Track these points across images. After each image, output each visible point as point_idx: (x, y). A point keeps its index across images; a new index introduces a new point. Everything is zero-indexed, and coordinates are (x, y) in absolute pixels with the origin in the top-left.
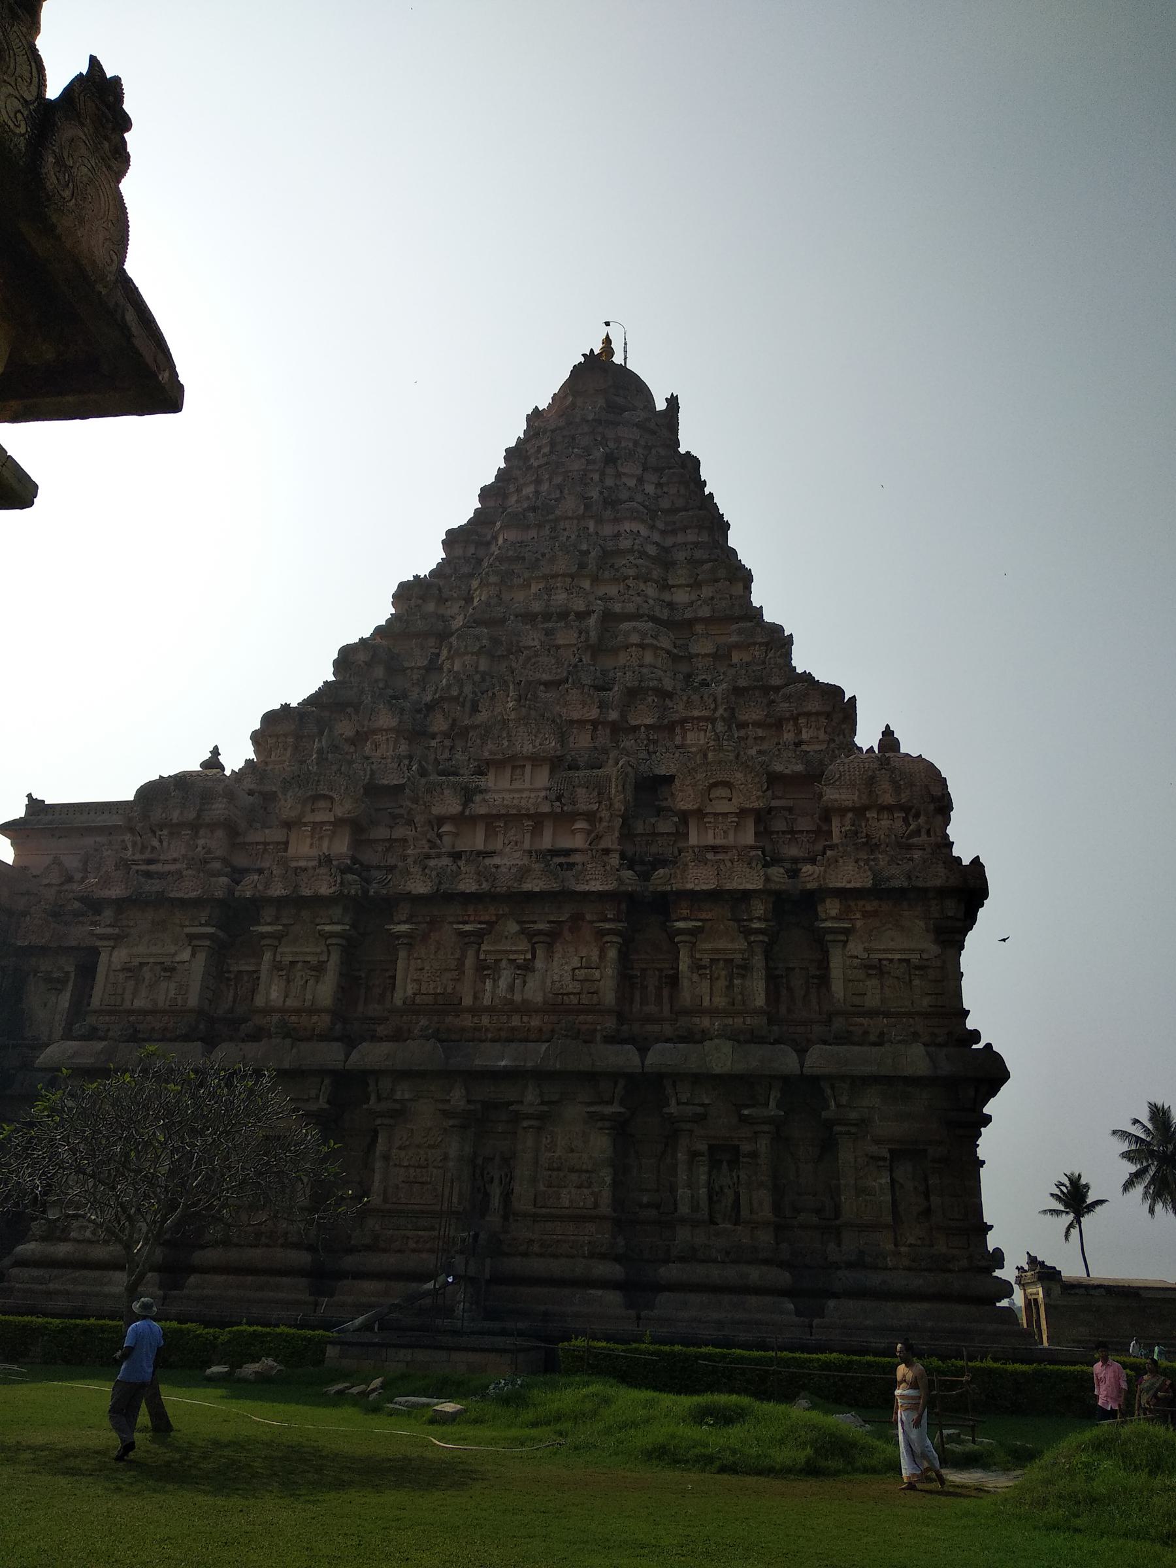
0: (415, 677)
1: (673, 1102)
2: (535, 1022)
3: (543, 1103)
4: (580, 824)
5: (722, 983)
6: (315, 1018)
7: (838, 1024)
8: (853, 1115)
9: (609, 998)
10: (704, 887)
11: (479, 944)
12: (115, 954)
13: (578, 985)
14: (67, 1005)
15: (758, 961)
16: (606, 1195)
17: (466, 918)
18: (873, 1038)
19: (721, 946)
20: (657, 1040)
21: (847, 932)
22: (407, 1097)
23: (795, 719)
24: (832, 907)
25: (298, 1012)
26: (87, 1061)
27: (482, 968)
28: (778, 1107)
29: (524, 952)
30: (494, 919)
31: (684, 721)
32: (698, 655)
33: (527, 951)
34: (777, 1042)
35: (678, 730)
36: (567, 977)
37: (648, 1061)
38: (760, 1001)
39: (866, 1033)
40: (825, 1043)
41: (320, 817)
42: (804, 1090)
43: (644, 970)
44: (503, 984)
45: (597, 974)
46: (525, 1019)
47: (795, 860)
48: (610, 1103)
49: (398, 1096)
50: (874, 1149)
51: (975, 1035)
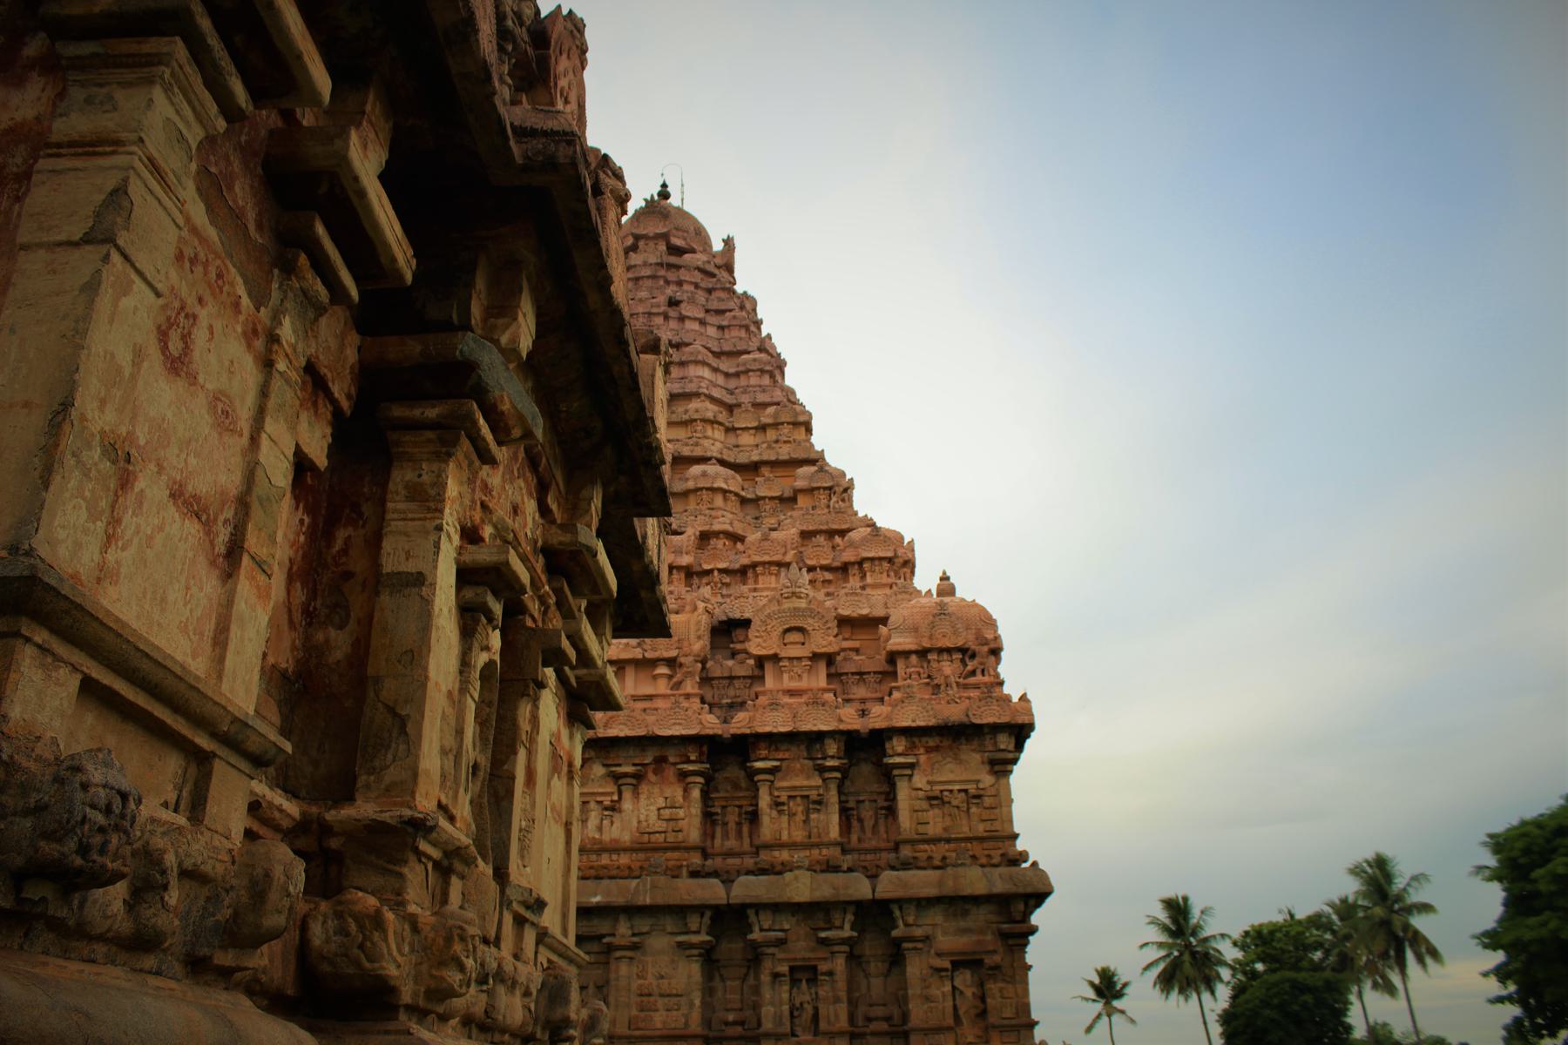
1: (757, 928)
2: (624, 859)
3: (634, 935)
4: (663, 670)
5: (800, 817)
7: (906, 852)
8: (918, 932)
9: (694, 834)
10: (782, 729)
13: (664, 824)
15: (833, 797)
16: (696, 1015)
18: (937, 862)
19: (797, 783)
20: (739, 873)
21: (912, 766)
23: (860, 563)
24: (899, 744)
28: (852, 929)
29: (612, 794)
31: (754, 566)
33: (612, 794)
34: (850, 870)
35: (750, 574)
36: (653, 817)
37: (733, 894)
38: (834, 833)
39: (930, 858)
40: (893, 868)
42: (875, 914)
43: (724, 807)
45: (681, 813)
46: (614, 857)
47: (863, 701)
48: (698, 932)
50: (938, 963)
51: (1023, 856)
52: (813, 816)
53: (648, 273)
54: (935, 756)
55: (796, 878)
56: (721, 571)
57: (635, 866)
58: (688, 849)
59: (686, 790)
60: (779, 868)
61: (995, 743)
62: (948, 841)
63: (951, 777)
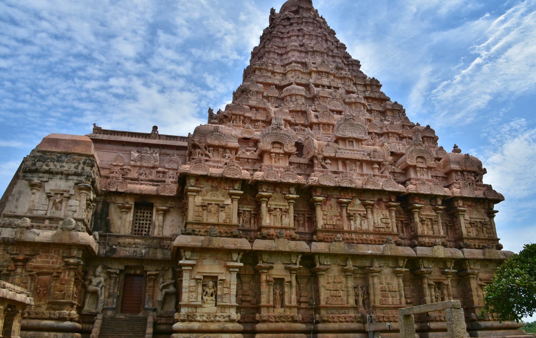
2: (372, 237)
3: (380, 267)
5: (430, 226)
6: (288, 231)
11: (347, 207)
12: (196, 198)
14: (132, 219)
18: (477, 247)
21: (464, 211)
24: (461, 203)
25: (282, 228)
26: (199, 244)
27: (349, 217)
32: (374, 110)
36: (380, 222)
37: (418, 253)
38: (442, 233)
39: (475, 245)
41: (277, 151)
44: (358, 222)
46: (368, 236)
48: (402, 267)
49: (325, 263)
50: (480, 282)
53: (311, 21)
54: (471, 209)
55: (438, 249)
56: (375, 133)
57: (377, 240)
59: (390, 212)
60: (427, 244)
61: (489, 206)
62: (479, 239)
63: (476, 217)
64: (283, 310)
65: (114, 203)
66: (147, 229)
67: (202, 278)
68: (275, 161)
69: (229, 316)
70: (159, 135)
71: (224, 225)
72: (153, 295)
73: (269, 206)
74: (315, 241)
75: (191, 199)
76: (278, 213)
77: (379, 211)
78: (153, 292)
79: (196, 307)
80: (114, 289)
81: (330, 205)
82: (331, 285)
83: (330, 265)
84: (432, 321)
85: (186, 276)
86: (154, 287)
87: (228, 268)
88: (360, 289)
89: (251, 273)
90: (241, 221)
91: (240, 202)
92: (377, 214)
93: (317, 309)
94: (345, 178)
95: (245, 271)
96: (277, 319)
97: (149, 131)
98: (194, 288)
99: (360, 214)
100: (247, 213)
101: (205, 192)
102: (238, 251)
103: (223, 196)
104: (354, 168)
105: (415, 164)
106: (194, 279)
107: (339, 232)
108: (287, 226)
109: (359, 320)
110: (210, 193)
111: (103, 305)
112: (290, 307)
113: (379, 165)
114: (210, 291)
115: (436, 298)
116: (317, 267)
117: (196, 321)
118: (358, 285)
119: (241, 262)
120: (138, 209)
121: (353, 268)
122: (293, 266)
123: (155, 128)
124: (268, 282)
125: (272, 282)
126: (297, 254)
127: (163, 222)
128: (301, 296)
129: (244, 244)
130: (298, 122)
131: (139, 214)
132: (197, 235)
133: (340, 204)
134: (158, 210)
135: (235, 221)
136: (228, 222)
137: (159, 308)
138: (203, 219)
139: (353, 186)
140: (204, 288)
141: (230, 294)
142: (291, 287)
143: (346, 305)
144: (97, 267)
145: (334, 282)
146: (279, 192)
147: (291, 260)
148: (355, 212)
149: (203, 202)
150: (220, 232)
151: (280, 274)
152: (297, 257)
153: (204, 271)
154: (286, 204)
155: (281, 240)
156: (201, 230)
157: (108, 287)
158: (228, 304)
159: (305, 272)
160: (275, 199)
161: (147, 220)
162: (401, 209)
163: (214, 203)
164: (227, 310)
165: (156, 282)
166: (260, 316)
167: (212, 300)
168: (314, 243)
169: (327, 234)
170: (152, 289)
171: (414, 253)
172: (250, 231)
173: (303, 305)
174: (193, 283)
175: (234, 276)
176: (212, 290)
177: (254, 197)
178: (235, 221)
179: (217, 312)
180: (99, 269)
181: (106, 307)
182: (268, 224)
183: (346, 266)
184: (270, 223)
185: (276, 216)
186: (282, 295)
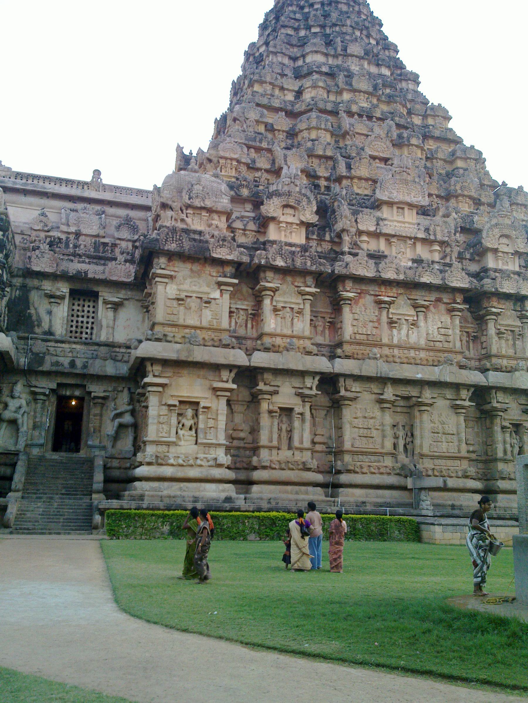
0: (281, 136)
2: (423, 355)
5: (511, 342)
6: (301, 342)
12: (168, 288)
17: (380, 293)
22: (358, 390)
25: (292, 337)
26: (173, 356)
27: (391, 323)
30: (395, 295)
36: (436, 333)
37: (490, 381)
41: (290, 219)
44: (404, 332)
46: (417, 353)
48: (465, 400)
49: (353, 390)
52: (517, 342)
55: (521, 375)
57: (430, 359)
58: (456, 352)
60: (504, 369)
64: (291, 452)
65: (38, 288)
66: (89, 331)
67: (177, 403)
68: (285, 235)
69: (216, 459)
70: (104, 185)
71: (209, 329)
72: (100, 427)
73: (274, 304)
74: (339, 357)
75: (160, 288)
76: (288, 314)
77: (437, 317)
78: (101, 423)
79: (168, 444)
80: (41, 417)
81: (364, 305)
82: (361, 420)
83: (359, 392)
84: (503, 479)
85: (153, 401)
86: (101, 415)
87: (215, 390)
88: (401, 428)
89: (248, 400)
90: (233, 324)
91: (233, 296)
92: (433, 321)
93: (338, 453)
94: (390, 265)
95: (238, 395)
96: (283, 466)
97: (88, 178)
98: (166, 417)
99: (407, 320)
100: (242, 312)
101: (181, 278)
102: (230, 367)
103: (208, 286)
104: (403, 250)
105: (496, 247)
106: (165, 404)
107: (375, 346)
108: (301, 334)
109: (398, 471)
110: (188, 281)
111: (26, 440)
112: (301, 450)
113: (441, 247)
114: (189, 423)
115: (511, 446)
116: (341, 394)
117: (168, 465)
118: (398, 423)
119: (234, 382)
120: (74, 299)
121: (393, 398)
122: (307, 392)
123: (97, 173)
124: (270, 412)
125: (276, 412)
126: (313, 374)
127: (114, 320)
128: (316, 435)
129: (239, 357)
130: (321, 175)
131: (76, 307)
132: (170, 342)
133: (379, 303)
134: (105, 302)
135: (225, 324)
136: (215, 324)
137: (109, 445)
138: (178, 319)
139: (402, 277)
140: (180, 418)
141: (217, 428)
142: (303, 421)
143: (381, 450)
144: (15, 383)
145: (365, 417)
146: (290, 283)
147: (304, 382)
148: (399, 317)
149: (178, 293)
150: (204, 339)
151: (287, 402)
152: (314, 379)
153: (180, 395)
154: (301, 301)
155: (292, 353)
156: (176, 335)
157: (32, 413)
158: (214, 441)
159: (324, 400)
160: (285, 293)
161: (88, 317)
162: (469, 314)
163: (194, 295)
164: (212, 451)
165: (105, 408)
166: (259, 461)
167: (192, 436)
168: (337, 360)
169: (358, 347)
170: (98, 417)
171: (485, 380)
172: (245, 338)
173: (318, 448)
174: (164, 410)
175: (223, 402)
176: (191, 422)
177: (253, 289)
178: (225, 324)
179: (197, 453)
180: (19, 388)
181: (29, 442)
182: (273, 330)
183: (382, 394)
184: (275, 329)
185: (284, 318)
186: (290, 431)
